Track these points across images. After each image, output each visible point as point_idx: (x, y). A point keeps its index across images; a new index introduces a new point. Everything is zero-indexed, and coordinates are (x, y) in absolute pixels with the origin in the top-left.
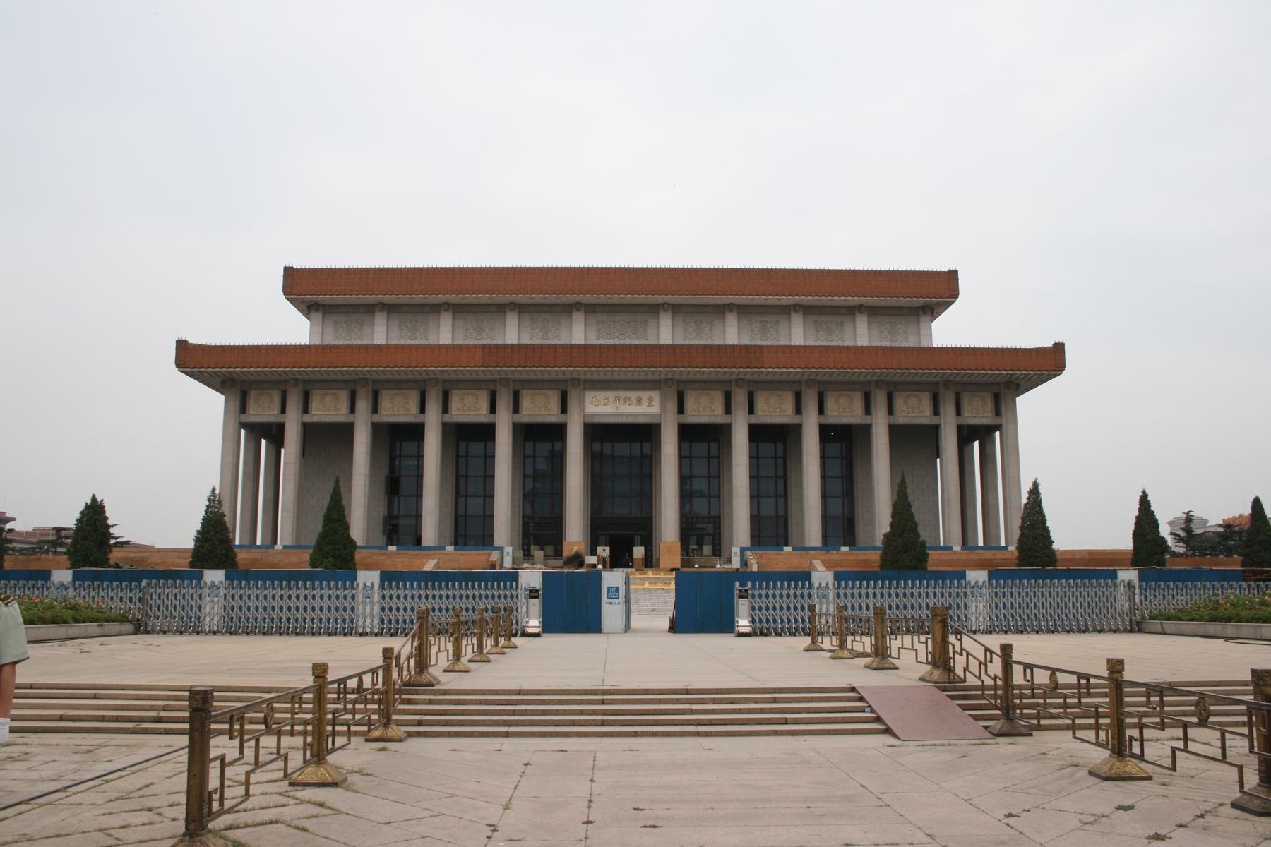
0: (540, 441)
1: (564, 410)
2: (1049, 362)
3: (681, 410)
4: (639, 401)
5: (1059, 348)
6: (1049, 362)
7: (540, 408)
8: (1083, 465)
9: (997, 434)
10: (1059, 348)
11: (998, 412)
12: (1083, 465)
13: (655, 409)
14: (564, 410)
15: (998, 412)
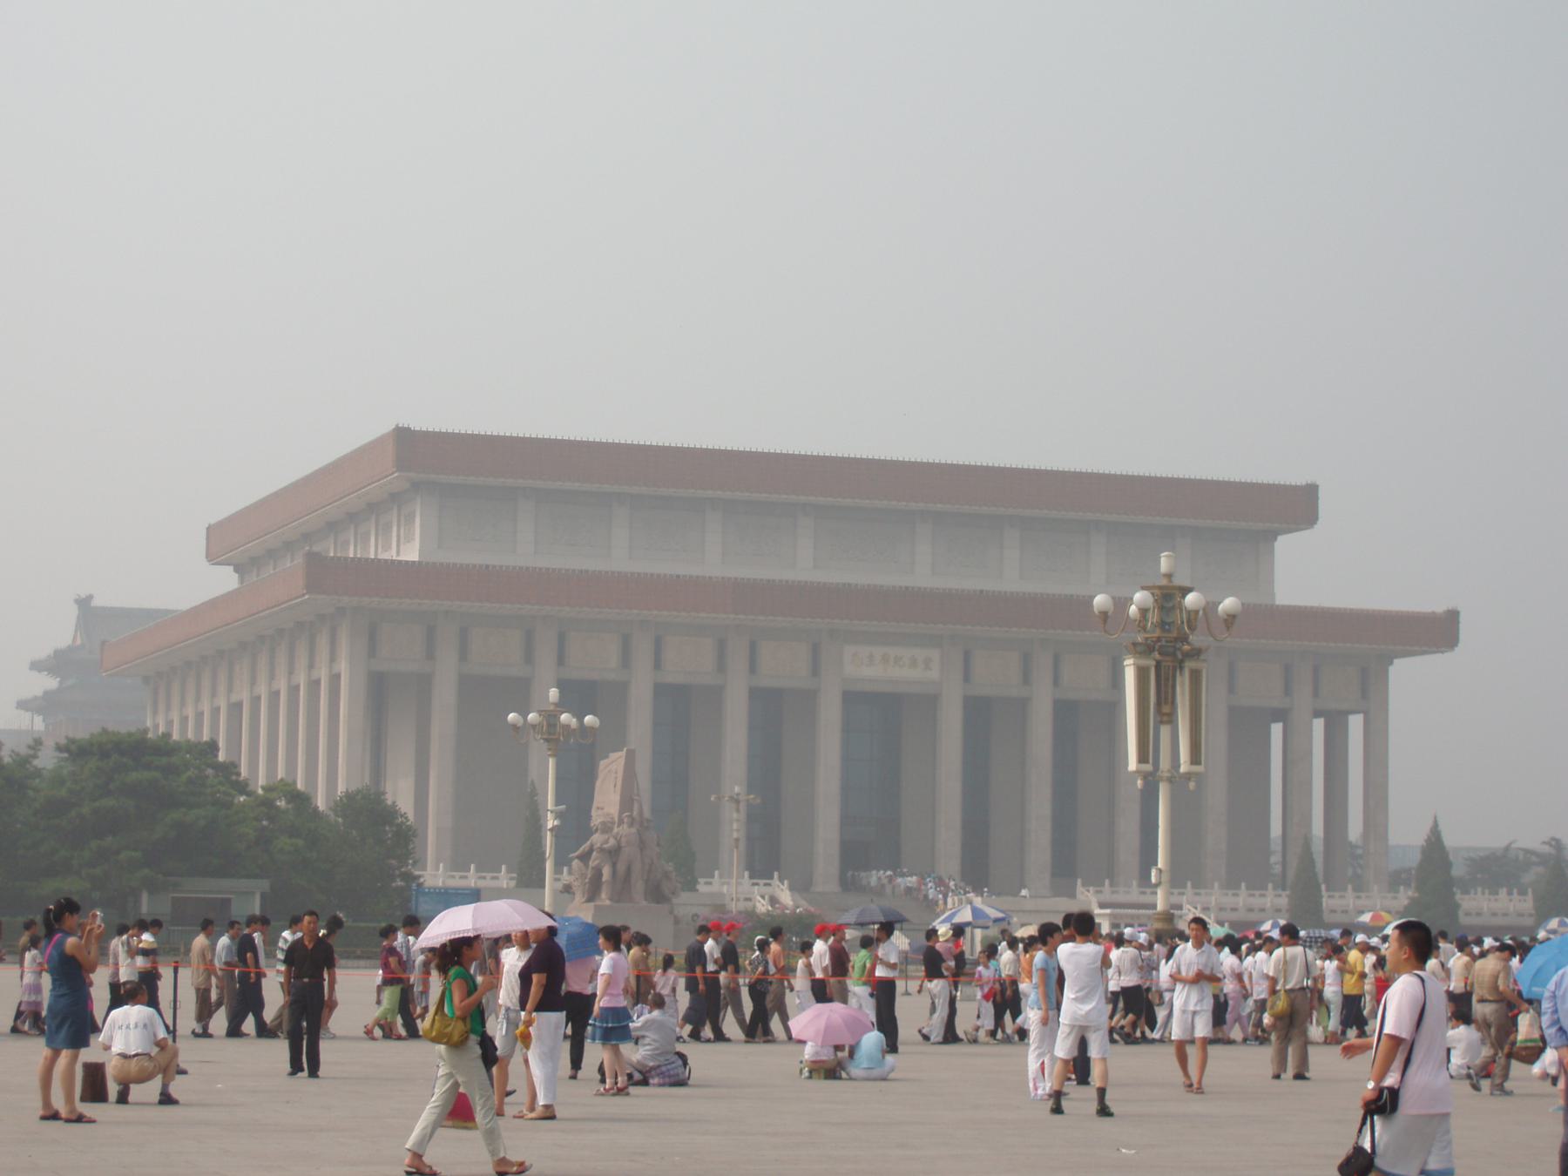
0: (776, 714)
1: (815, 671)
2: (1436, 632)
3: (967, 678)
4: (914, 663)
5: (1452, 617)
6: (1436, 632)
7: (784, 665)
8: (1455, 767)
9: (1356, 723)
10: (1452, 617)
11: (1364, 694)
12: (1455, 767)
13: (934, 674)
14: (815, 671)
15: (1364, 694)
